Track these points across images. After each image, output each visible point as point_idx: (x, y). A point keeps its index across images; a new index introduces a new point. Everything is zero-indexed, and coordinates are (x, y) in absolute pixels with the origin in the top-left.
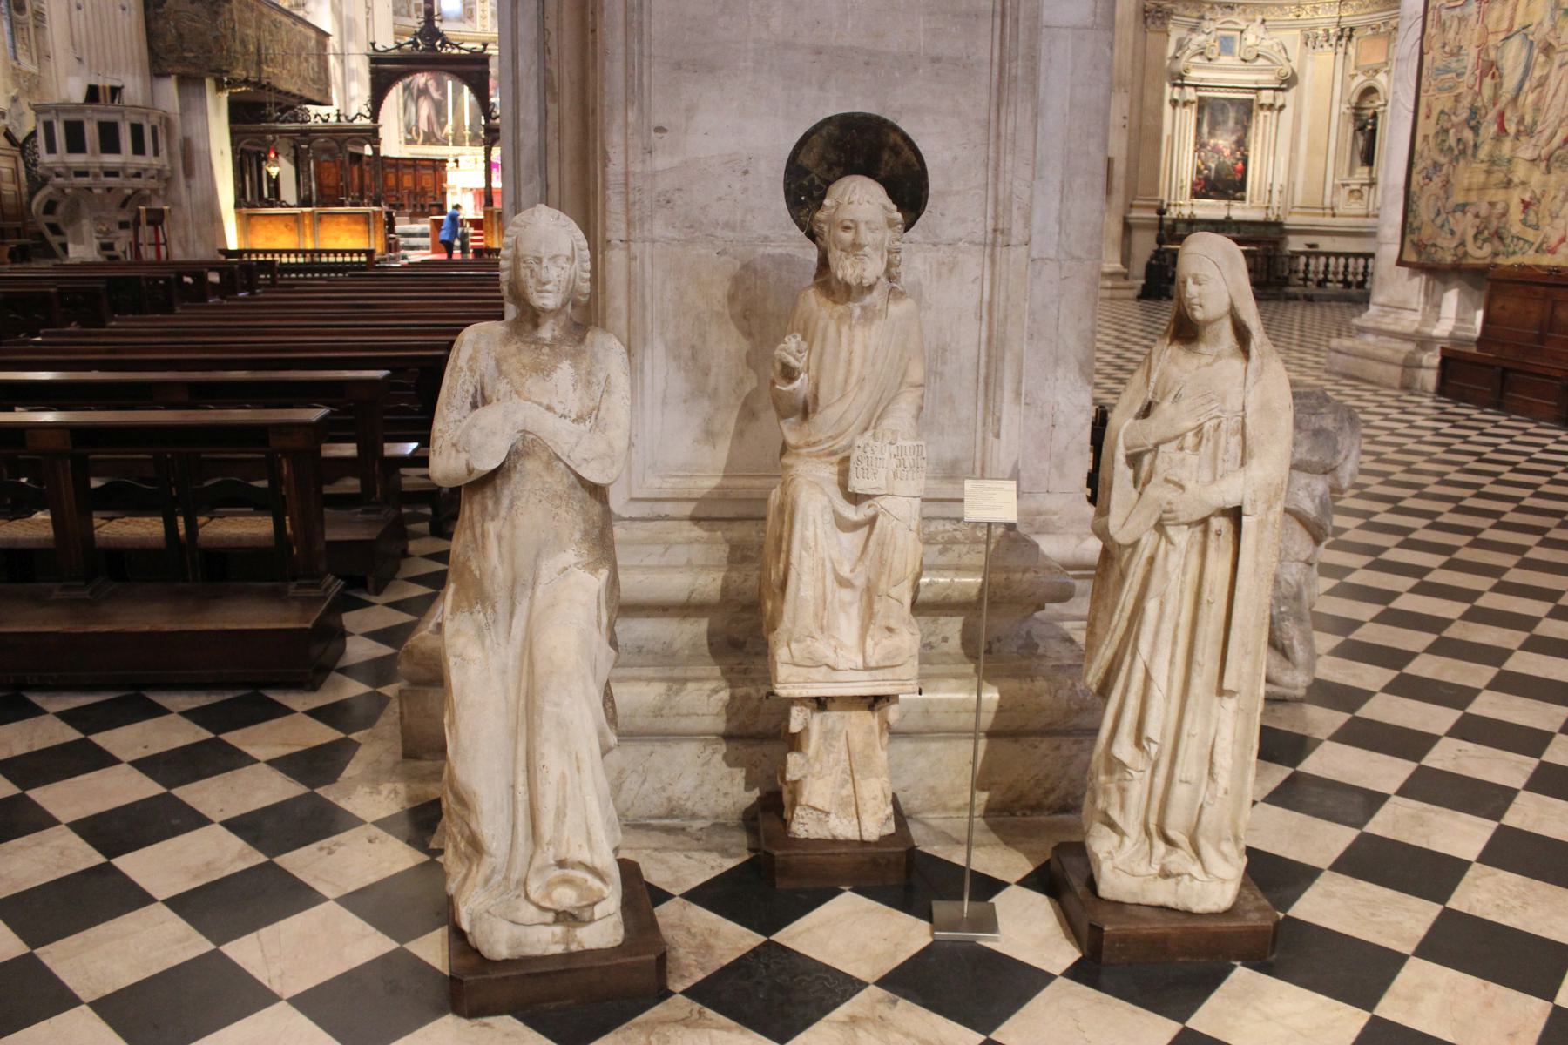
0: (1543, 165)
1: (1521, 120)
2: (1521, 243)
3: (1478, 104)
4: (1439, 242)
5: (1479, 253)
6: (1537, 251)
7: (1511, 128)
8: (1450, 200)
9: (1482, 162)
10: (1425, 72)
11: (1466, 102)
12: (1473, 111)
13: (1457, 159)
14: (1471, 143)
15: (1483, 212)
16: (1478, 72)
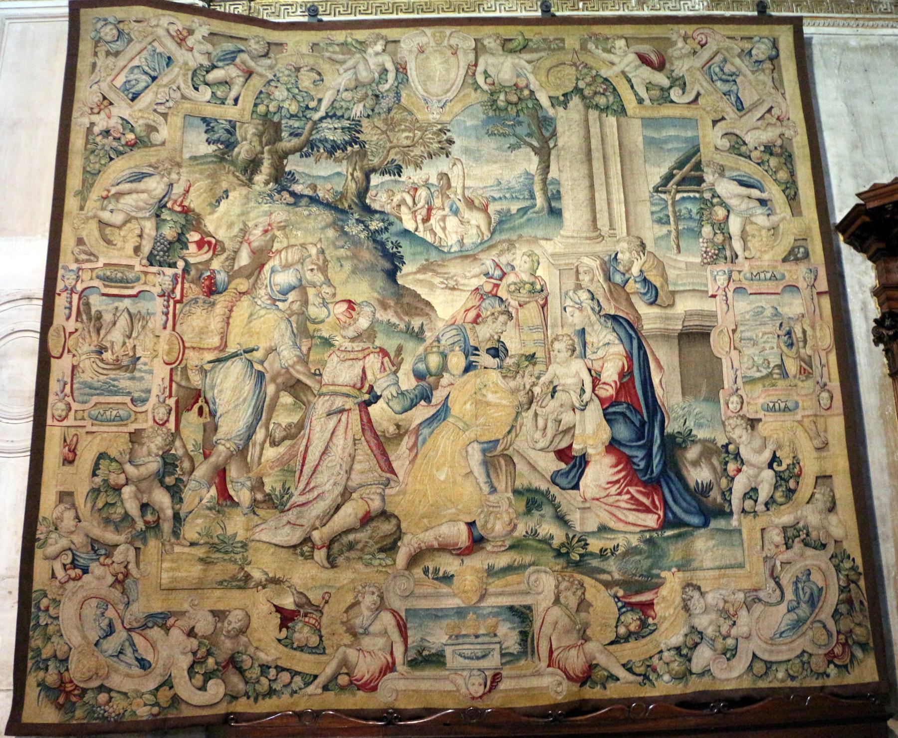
0: (320, 555)
1: (259, 485)
2: (285, 677)
3: (178, 450)
4: (116, 681)
5: (199, 698)
6: (325, 688)
7: (243, 496)
8: (134, 607)
9: (192, 544)
10: (54, 386)
11: (155, 443)
12: (169, 463)
13: (142, 536)
14: (169, 513)
15: (204, 624)
16: (172, 402)
